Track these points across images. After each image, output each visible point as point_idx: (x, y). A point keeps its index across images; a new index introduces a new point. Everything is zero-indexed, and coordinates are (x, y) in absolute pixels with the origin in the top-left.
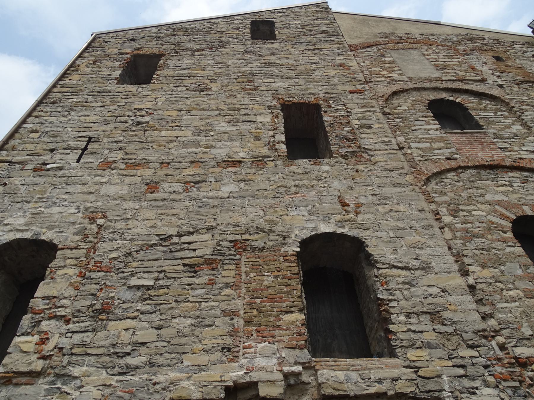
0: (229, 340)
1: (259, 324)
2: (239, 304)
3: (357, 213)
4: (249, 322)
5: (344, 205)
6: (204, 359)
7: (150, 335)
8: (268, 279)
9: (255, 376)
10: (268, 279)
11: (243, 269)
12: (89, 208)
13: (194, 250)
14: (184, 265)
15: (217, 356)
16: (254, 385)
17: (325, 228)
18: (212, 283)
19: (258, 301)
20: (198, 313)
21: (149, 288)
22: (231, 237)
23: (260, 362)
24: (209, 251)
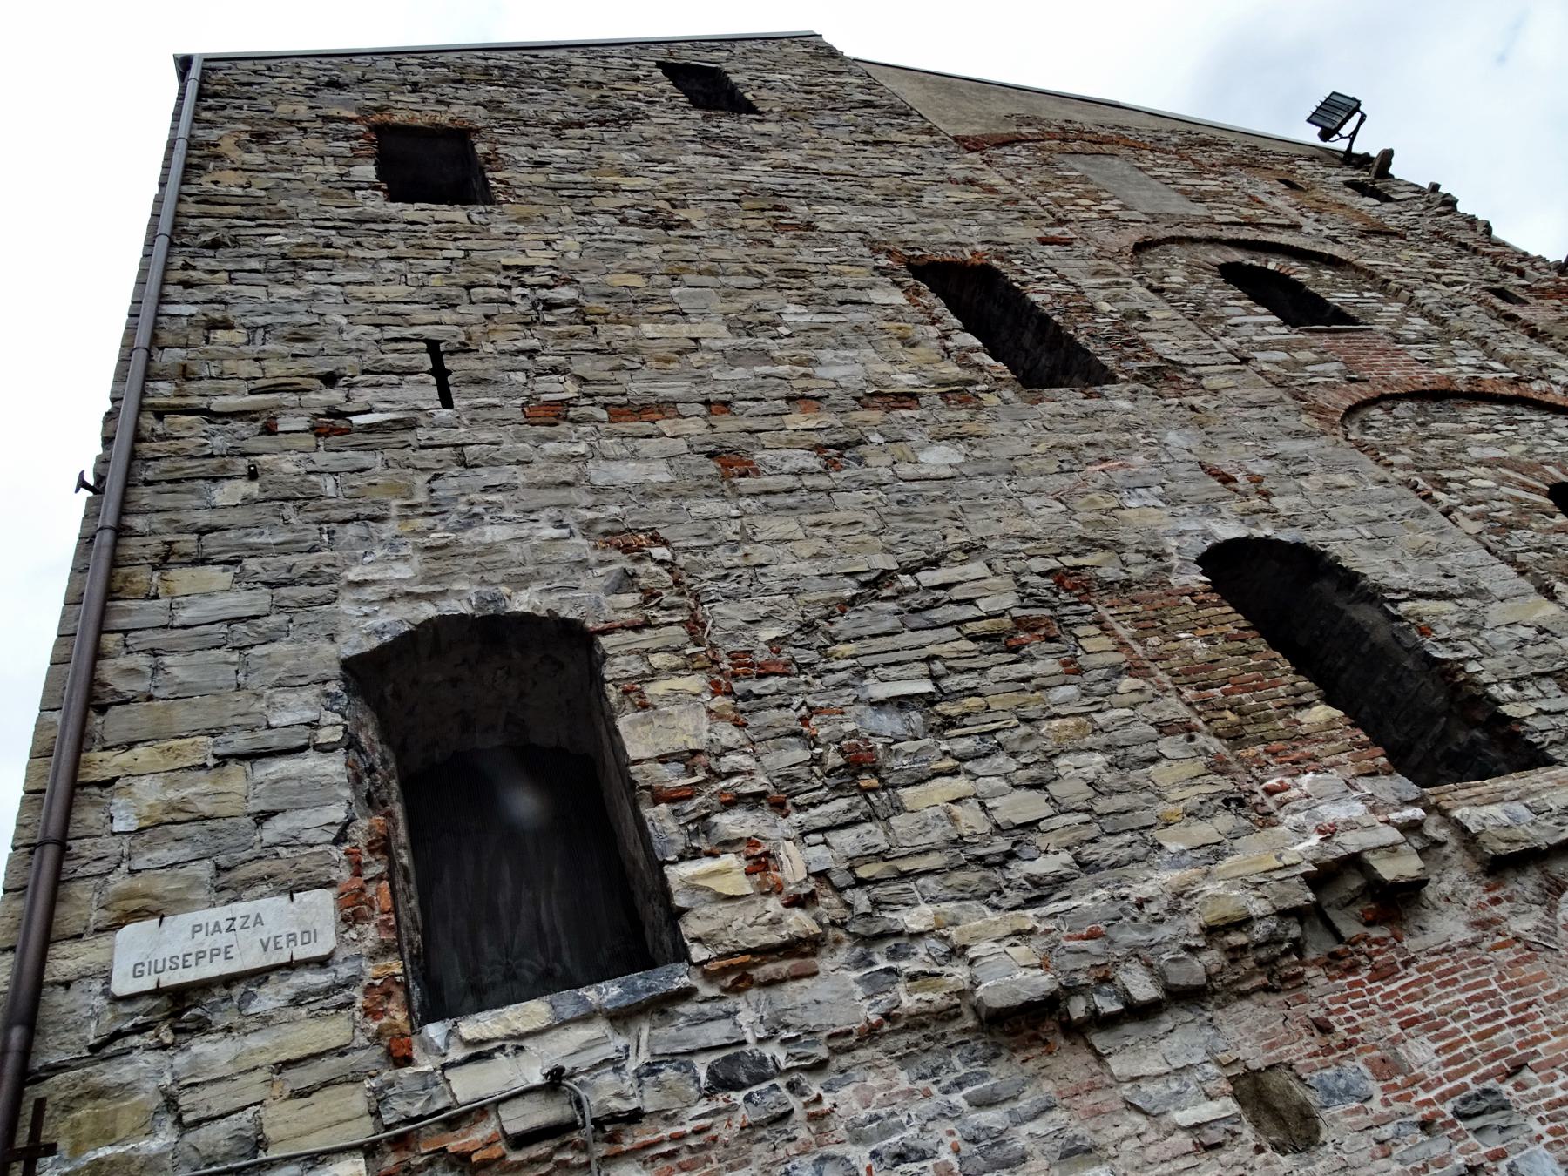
7: (1029, 806)
12: (595, 521)
13: (971, 602)
14: (974, 638)
20: (1103, 739)
21: (929, 700)
22: (1038, 565)
24: (1009, 601)
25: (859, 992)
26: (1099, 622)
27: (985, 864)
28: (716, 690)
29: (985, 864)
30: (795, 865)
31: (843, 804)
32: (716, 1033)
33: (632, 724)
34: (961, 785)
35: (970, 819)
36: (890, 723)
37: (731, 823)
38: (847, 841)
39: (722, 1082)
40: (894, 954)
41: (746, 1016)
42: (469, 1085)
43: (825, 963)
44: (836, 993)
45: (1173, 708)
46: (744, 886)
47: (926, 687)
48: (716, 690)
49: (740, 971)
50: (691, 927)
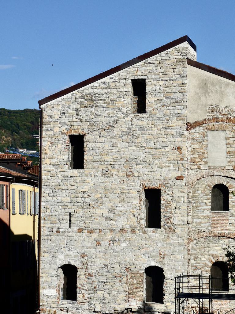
0: (125, 298)
1: (131, 293)
2: (127, 289)
3: (164, 258)
4: (130, 294)
5: (160, 254)
6: (120, 302)
7: (108, 295)
8: (135, 282)
9: (131, 307)
10: (135, 282)
11: (128, 278)
13: (115, 270)
15: (123, 302)
16: (131, 309)
17: (153, 264)
18: (120, 282)
19: (132, 288)
23: (132, 304)
24: (119, 271)
25: (87, 306)
26: (127, 276)
27: (101, 300)
28: (86, 277)
29: (101, 300)
30: (87, 296)
31: (92, 291)
32: (77, 307)
33: (78, 280)
34: (103, 292)
35: (102, 296)
36: (100, 284)
37: (83, 291)
38: (91, 295)
39: (77, 309)
40: (91, 305)
41: (79, 306)
42: (62, 306)
43: (85, 304)
44: (86, 306)
45: (127, 289)
46: (82, 297)
47: (105, 281)
48: (86, 277)
49: (79, 303)
50: (77, 300)
